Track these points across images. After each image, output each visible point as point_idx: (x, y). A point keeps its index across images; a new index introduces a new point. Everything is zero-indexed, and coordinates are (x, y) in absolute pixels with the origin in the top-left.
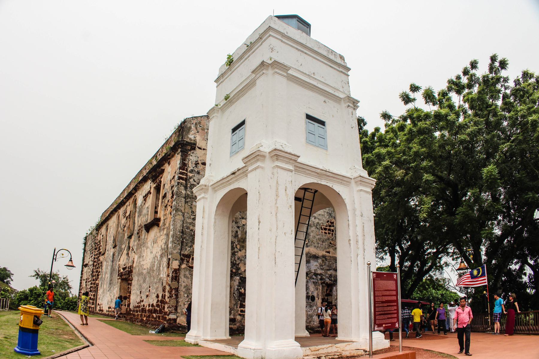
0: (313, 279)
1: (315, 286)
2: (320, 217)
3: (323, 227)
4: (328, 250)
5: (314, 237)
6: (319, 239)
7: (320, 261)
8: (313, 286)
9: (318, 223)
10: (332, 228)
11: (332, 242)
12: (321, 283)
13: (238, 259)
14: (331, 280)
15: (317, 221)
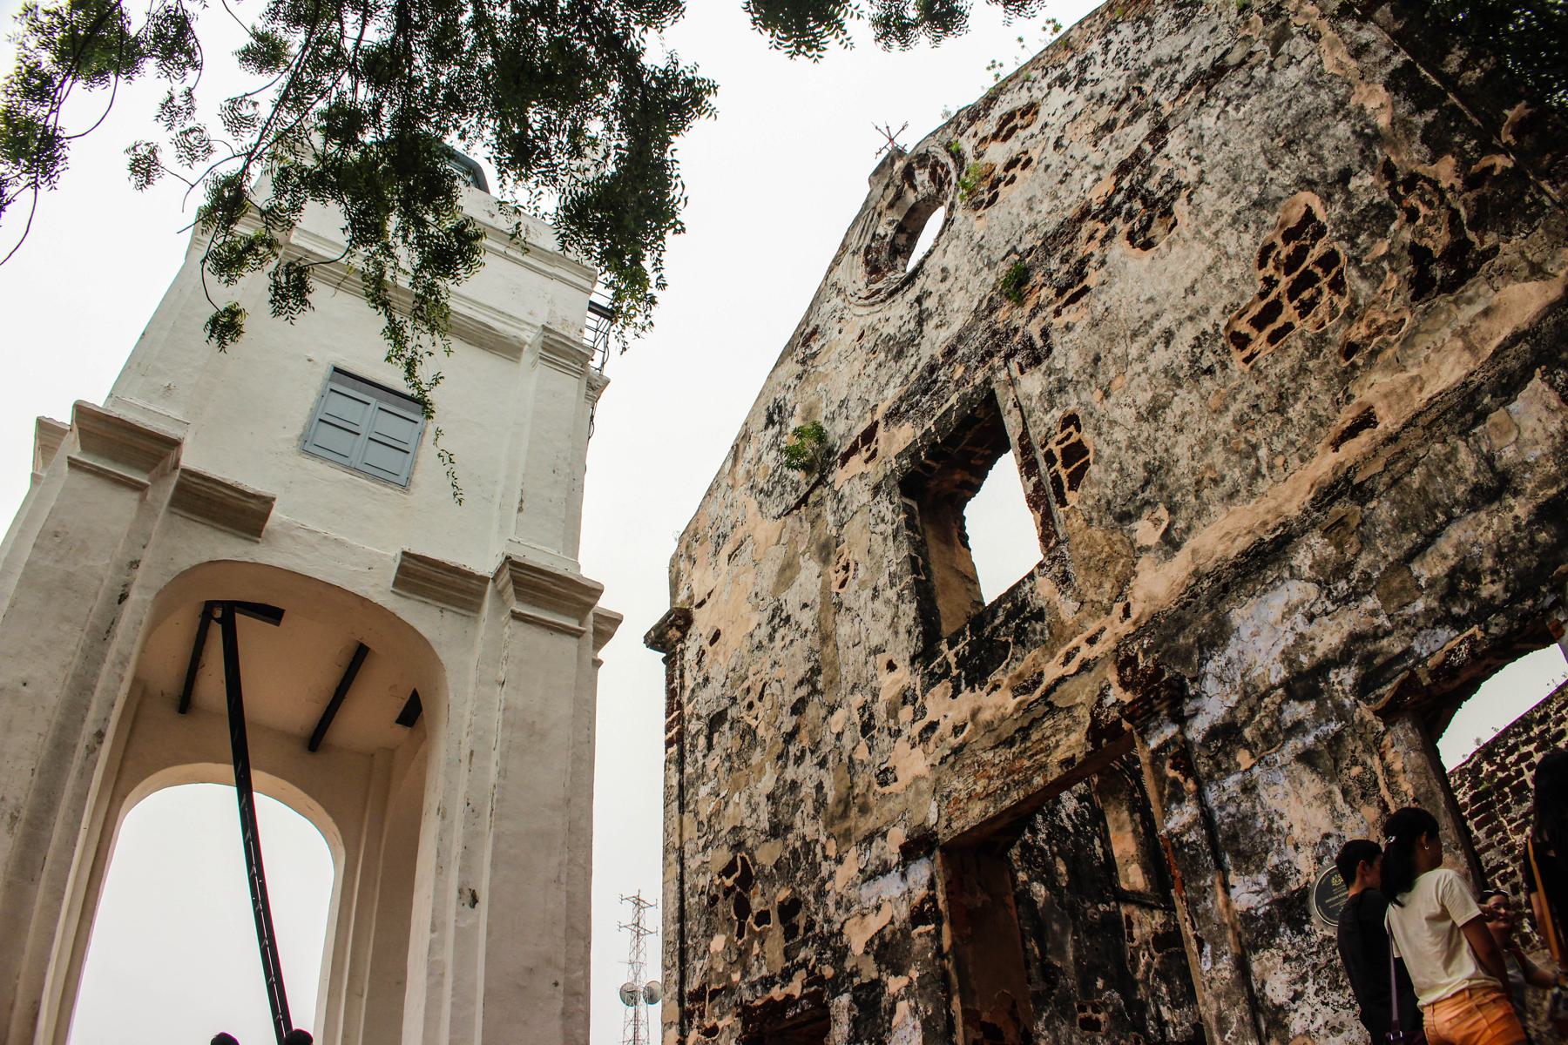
0: (1298, 727)
1: (1332, 774)
2: (1196, 301)
3: (1243, 327)
4: (1346, 417)
5: (1205, 445)
6: (1240, 422)
7: (1311, 551)
8: (1312, 784)
9: (1199, 341)
10: (1317, 251)
11: (1358, 332)
12: (1389, 714)
13: (838, 904)
14: (1484, 611)
15: (1186, 335)
